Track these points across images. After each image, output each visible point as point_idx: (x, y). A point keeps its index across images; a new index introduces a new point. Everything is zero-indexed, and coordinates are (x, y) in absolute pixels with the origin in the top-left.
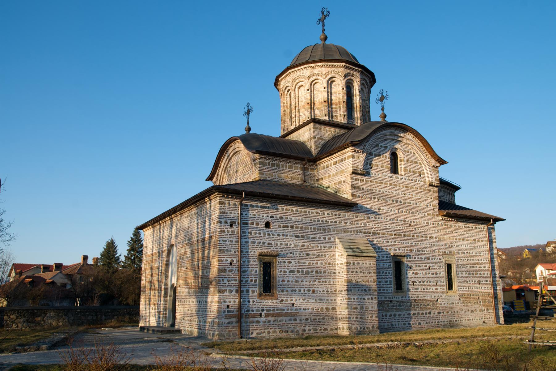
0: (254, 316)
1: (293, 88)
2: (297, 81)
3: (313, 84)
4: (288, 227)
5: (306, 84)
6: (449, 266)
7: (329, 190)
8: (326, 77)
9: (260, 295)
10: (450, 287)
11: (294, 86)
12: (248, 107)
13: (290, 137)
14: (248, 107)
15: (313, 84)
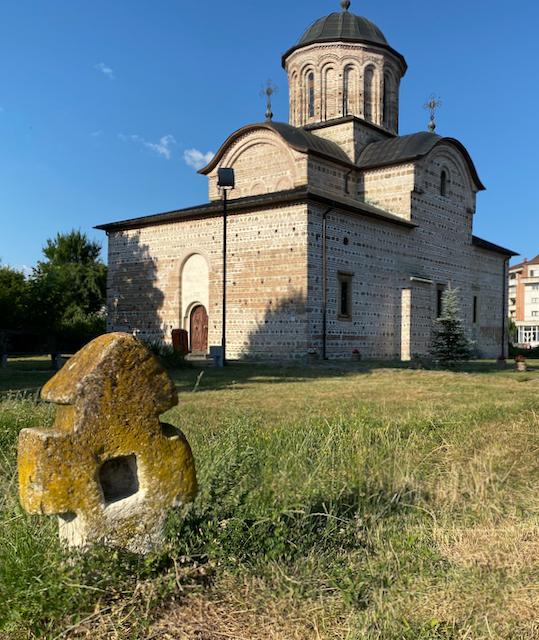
0: (335, 338)
1: (319, 68)
2: (325, 61)
3: (348, 68)
4: (359, 245)
5: (339, 68)
6: (475, 298)
7: (377, 207)
8: (364, 62)
9: (339, 316)
10: (474, 321)
11: (321, 65)
12: (269, 84)
13: (319, 133)
14: (269, 84)
15: (348, 68)
